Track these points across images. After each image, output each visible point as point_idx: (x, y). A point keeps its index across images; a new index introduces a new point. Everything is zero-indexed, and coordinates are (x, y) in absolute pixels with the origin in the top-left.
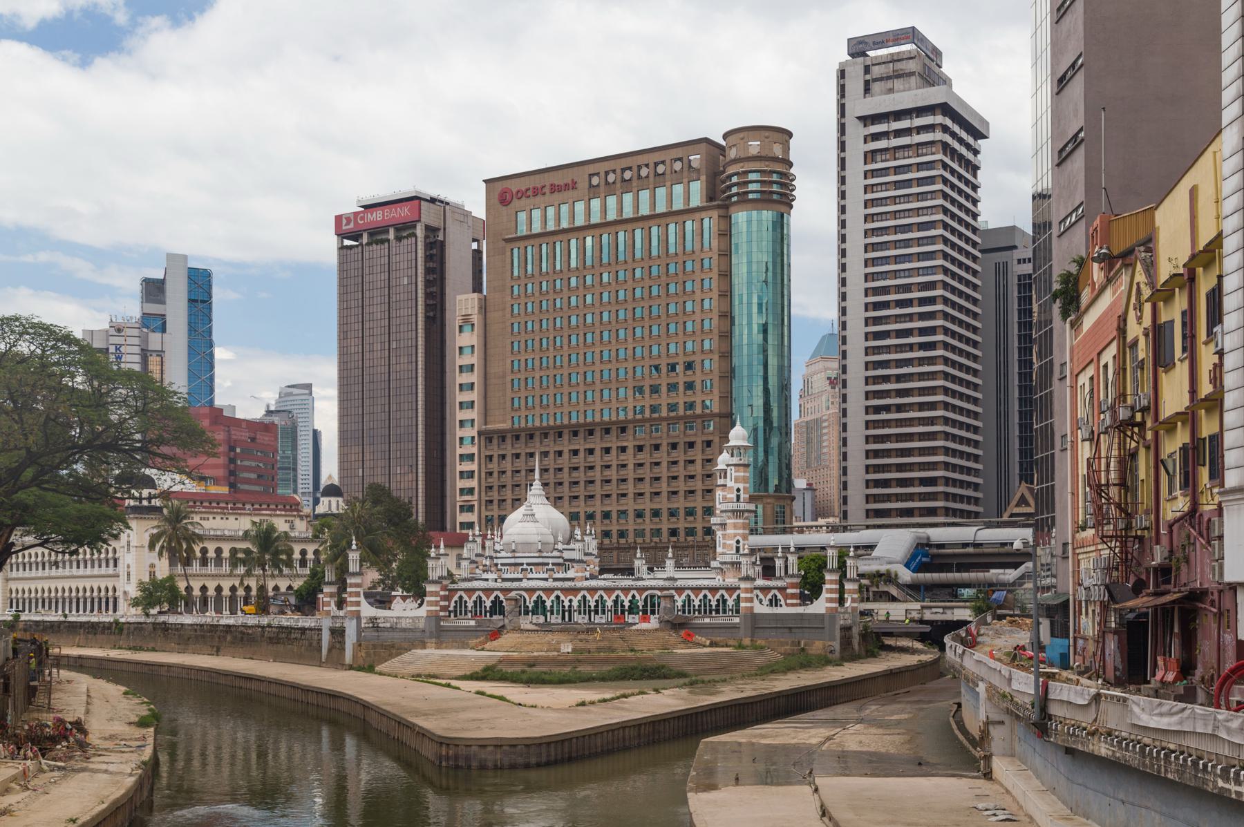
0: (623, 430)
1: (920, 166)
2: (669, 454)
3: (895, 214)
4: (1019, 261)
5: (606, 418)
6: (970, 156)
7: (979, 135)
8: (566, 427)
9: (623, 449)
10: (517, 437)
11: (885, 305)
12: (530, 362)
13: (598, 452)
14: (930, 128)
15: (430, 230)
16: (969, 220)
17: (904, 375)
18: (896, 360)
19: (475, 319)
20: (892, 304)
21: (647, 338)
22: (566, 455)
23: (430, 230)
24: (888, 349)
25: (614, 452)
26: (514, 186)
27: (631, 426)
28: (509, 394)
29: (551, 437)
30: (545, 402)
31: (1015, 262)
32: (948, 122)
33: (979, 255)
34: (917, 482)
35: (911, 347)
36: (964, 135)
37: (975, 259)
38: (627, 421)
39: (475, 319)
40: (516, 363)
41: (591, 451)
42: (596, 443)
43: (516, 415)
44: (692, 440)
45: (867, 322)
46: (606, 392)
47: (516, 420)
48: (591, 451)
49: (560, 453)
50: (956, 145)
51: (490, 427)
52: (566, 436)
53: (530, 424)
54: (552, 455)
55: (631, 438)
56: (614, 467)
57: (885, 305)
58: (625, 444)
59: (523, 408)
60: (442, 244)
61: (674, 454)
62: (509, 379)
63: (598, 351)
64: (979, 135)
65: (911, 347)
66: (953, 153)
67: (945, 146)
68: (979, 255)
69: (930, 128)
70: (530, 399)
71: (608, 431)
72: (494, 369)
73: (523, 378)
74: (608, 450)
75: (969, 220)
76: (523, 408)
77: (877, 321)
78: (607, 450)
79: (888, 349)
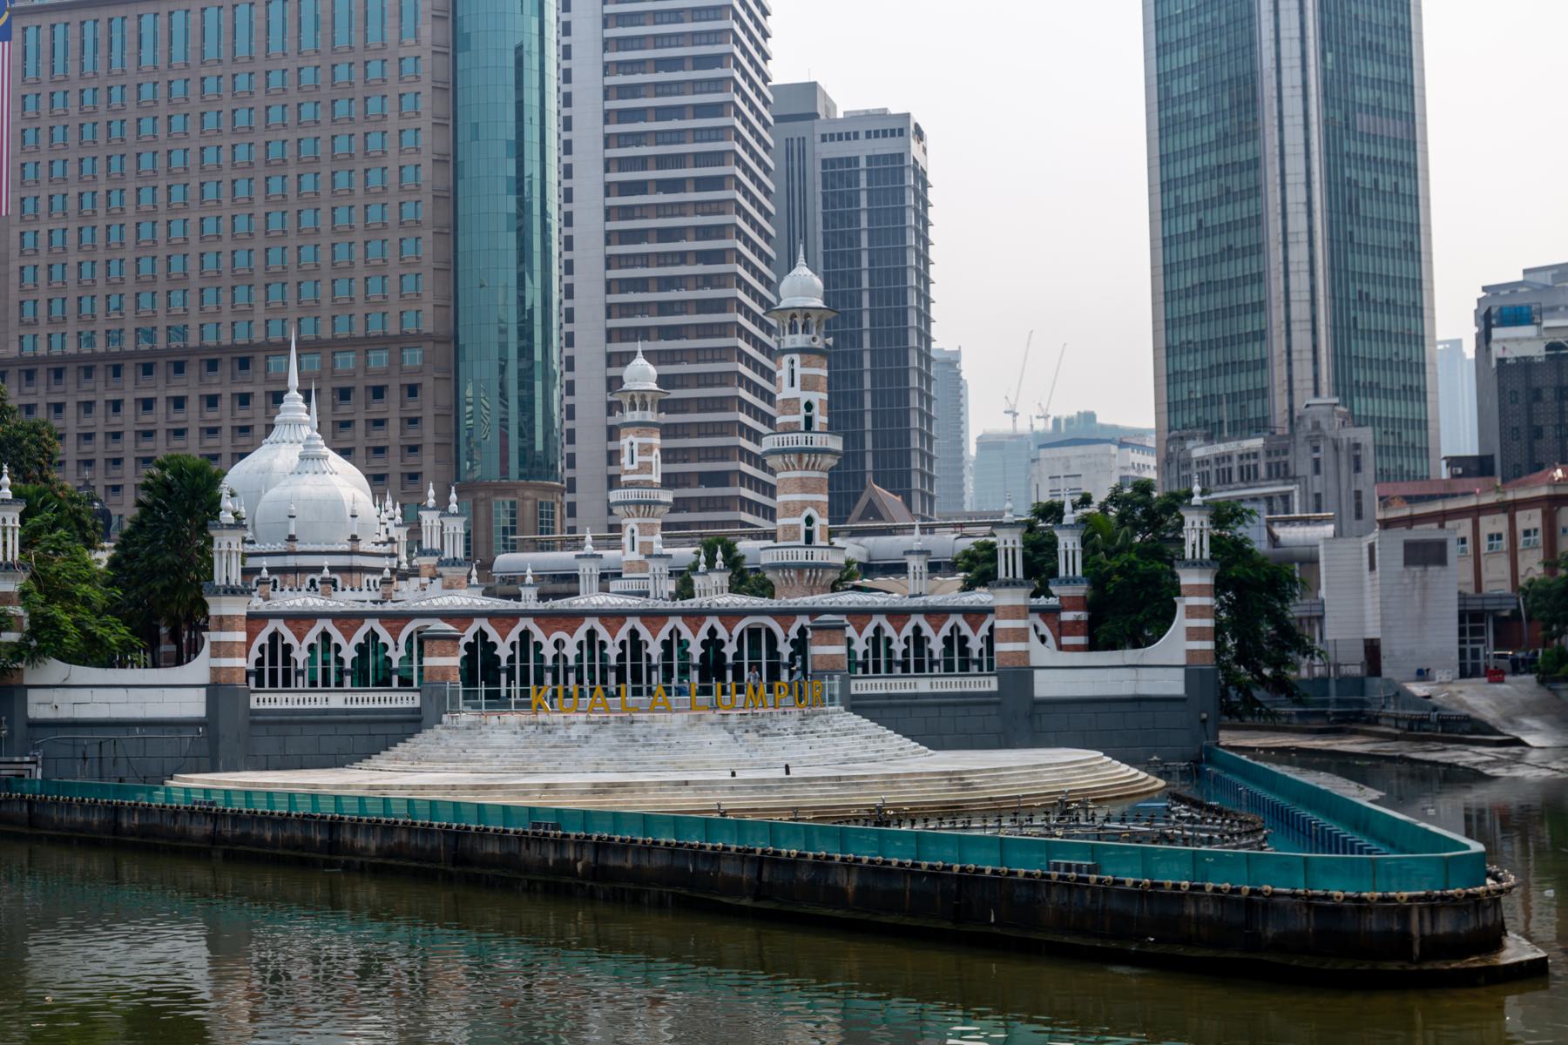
0: (244, 364)
2: (334, 407)
3: (658, 41)
4: (824, 138)
5: (210, 341)
8: (130, 355)
9: (244, 399)
10: (30, 375)
11: (640, 187)
12: (57, 237)
13: (193, 405)
16: (758, 58)
17: (672, 303)
18: (658, 278)
20: (652, 187)
21: (292, 197)
22: (128, 409)
24: (645, 260)
25: (225, 403)
27: (261, 356)
28: (14, 294)
29: (100, 375)
30: (86, 309)
31: (818, 138)
33: (771, 120)
34: (695, 480)
35: (682, 258)
37: (766, 125)
38: (251, 346)
40: (29, 238)
41: (179, 403)
42: (191, 386)
43: (28, 334)
44: (380, 382)
45: (609, 213)
46: (210, 295)
47: (28, 342)
48: (179, 403)
49: (116, 406)
52: (129, 374)
53: (56, 350)
54: (100, 408)
55: (260, 377)
56: (226, 432)
57: (640, 187)
58: (247, 389)
59: (43, 319)
61: (345, 408)
62: (14, 266)
63: (194, 218)
65: (682, 258)
68: (771, 120)
70: (57, 305)
71: (213, 365)
73: (43, 264)
74: (212, 401)
75: (758, 58)
76: (43, 319)
77: (627, 212)
78: (212, 401)
79: (645, 260)
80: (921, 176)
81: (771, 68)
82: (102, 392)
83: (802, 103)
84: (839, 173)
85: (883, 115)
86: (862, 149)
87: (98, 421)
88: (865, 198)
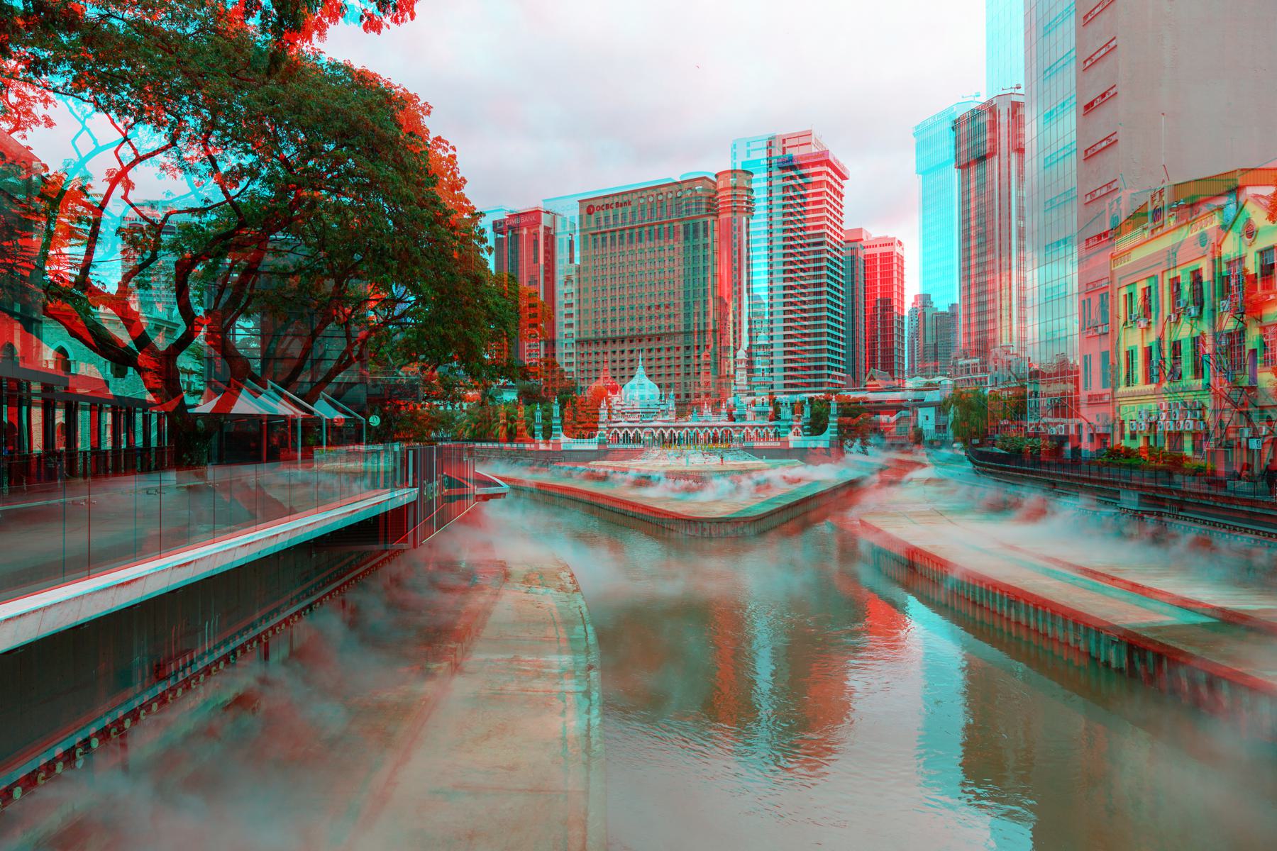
1: (814, 195)
6: (839, 188)
7: (844, 178)
14: (820, 173)
15: (547, 229)
19: (574, 278)
22: (626, 353)
23: (547, 229)
26: (596, 204)
32: (830, 170)
36: (836, 177)
39: (574, 278)
49: (623, 352)
50: (833, 183)
51: (583, 336)
60: (553, 237)
64: (844, 178)
66: (832, 187)
67: (828, 183)
69: (820, 173)
72: (583, 306)
80: (901, 259)
81: (845, 226)
82: (618, 348)
83: (855, 240)
84: (870, 259)
85: (886, 238)
86: (878, 251)
87: (618, 357)
88: (881, 267)
